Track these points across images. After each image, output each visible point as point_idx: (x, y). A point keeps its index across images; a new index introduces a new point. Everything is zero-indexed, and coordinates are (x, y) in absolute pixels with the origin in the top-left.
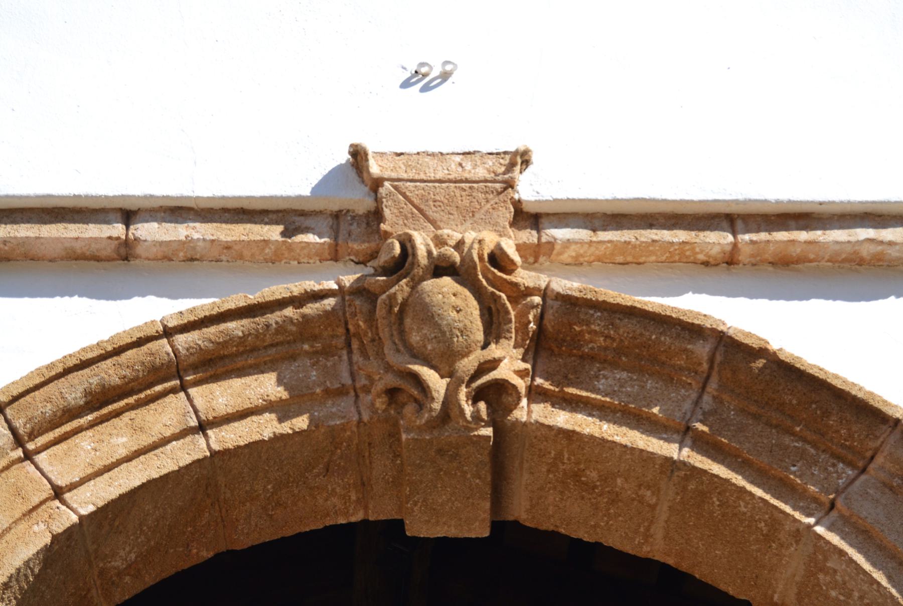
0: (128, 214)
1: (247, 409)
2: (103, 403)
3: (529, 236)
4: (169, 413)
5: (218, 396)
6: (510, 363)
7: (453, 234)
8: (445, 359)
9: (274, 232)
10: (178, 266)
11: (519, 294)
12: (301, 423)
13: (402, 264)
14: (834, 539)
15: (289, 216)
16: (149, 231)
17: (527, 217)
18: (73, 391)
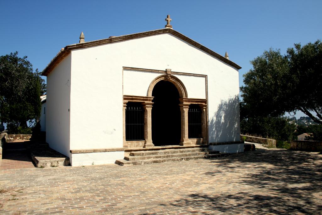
0: (159, 71)
1: (163, 79)
2: (157, 79)
4: (160, 79)
17: (171, 72)
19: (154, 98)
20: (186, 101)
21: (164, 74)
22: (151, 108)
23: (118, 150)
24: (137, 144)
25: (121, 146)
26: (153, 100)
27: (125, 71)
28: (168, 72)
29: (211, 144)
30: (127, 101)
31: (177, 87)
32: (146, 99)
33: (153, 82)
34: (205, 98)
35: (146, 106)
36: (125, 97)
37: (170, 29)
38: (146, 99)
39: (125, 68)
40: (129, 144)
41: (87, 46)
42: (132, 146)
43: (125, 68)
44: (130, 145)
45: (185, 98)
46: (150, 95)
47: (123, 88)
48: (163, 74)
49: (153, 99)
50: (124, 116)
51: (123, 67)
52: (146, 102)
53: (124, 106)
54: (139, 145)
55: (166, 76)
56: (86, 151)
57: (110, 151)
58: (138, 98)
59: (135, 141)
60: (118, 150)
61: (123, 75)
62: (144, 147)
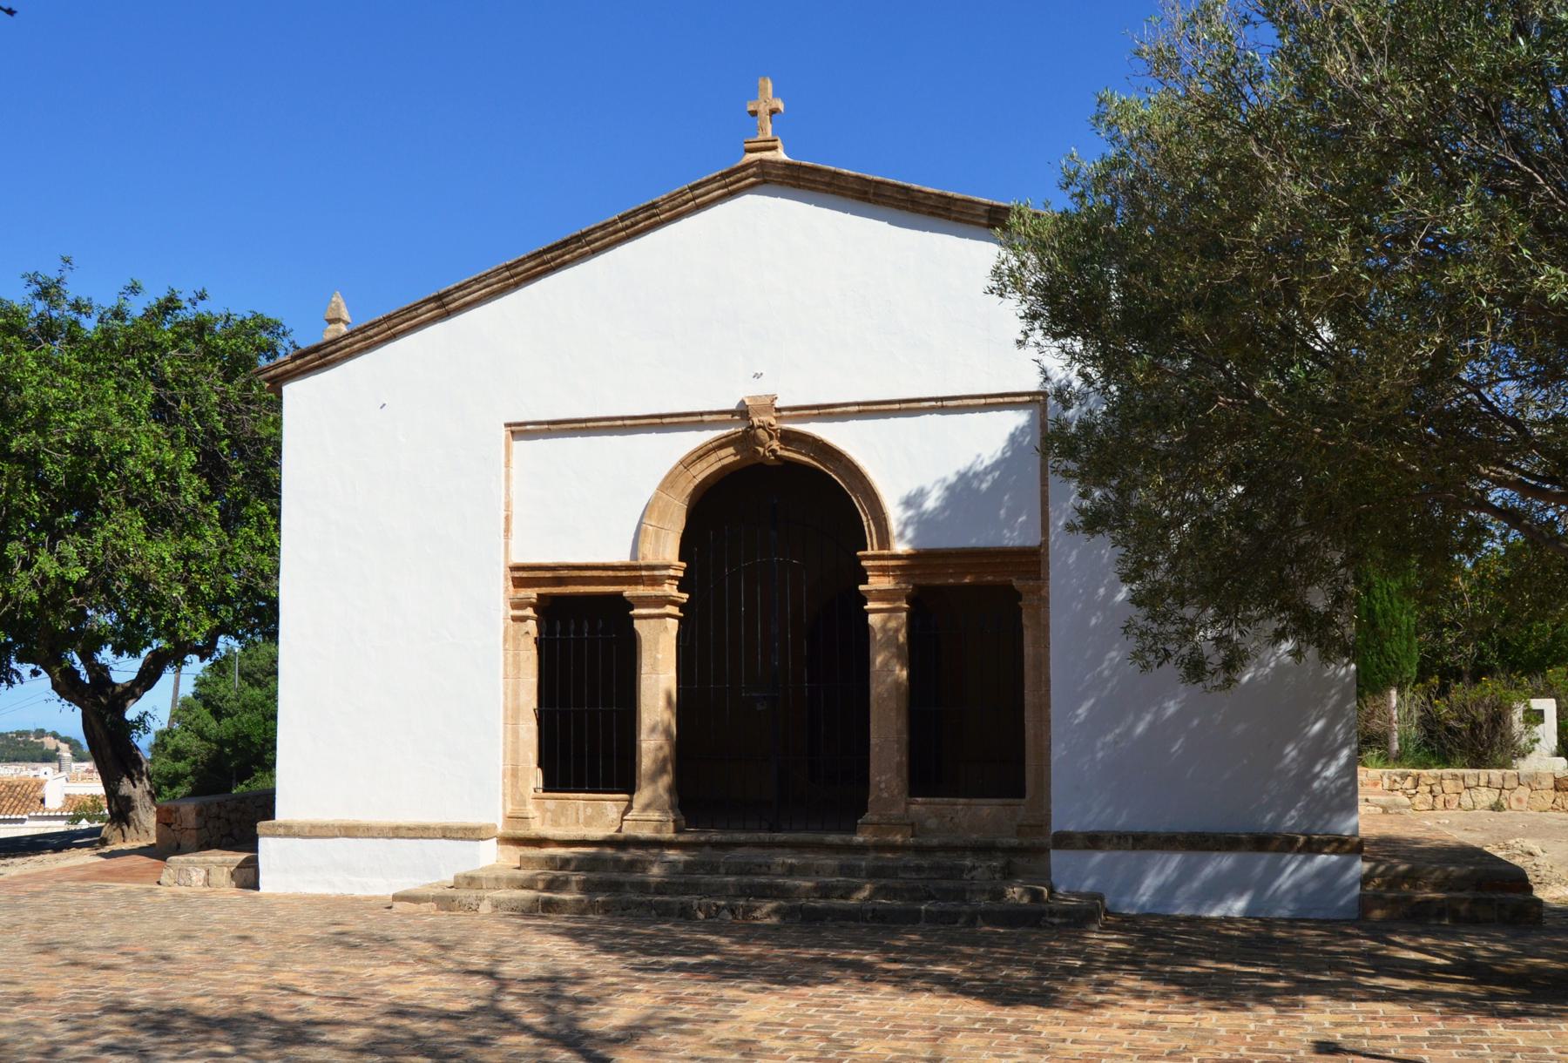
0: (701, 414)
1: (728, 456)
2: (700, 457)
4: (713, 457)
5: (722, 453)
6: (775, 444)
8: (762, 445)
9: (729, 417)
13: (752, 427)
15: (732, 413)
16: (706, 418)
17: (778, 410)
20: (884, 571)
21: (733, 430)
24: (589, 810)
27: (520, 446)
30: (532, 593)
33: (669, 483)
34: (1033, 540)
36: (517, 574)
37: (761, 160)
39: (520, 431)
42: (563, 820)
43: (520, 431)
45: (876, 552)
47: (507, 530)
48: (725, 432)
52: (629, 591)
53: (515, 619)
54: (601, 814)
55: (746, 441)
56: (313, 827)
57: (404, 833)
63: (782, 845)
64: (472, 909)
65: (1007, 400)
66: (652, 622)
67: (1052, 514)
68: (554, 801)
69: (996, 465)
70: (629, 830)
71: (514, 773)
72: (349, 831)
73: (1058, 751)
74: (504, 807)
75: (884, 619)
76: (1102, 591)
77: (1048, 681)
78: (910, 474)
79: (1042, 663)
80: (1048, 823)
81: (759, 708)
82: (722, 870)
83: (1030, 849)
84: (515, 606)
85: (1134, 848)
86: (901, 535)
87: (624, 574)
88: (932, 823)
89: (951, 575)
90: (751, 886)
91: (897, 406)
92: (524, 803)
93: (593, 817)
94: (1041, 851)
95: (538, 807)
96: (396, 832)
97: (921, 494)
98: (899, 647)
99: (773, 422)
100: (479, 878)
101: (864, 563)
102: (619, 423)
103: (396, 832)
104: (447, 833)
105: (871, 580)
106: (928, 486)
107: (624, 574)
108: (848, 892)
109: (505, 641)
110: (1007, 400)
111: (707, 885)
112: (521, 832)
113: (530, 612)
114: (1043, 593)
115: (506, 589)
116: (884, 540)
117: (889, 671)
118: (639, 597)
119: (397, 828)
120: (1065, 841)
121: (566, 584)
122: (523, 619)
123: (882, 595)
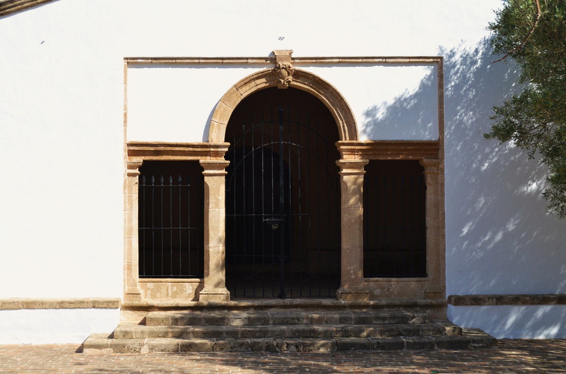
0: (247, 59)
1: (262, 83)
3: (293, 61)
4: (253, 84)
5: (258, 82)
6: (290, 78)
7: (284, 63)
8: (283, 79)
9: (264, 61)
10: (253, 65)
11: (291, 70)
12: (268, 84)
13: (279, 68)
14: (324, 98)
16: (250, 61)
17: (293, 59)
18: (243, 83)
19: (230, 148)
20: (352, 152)
21: (265, 69)
22: (223, 178)
23: (110, 305)
24: (175, 289)
25: (118, 293)
26: (226, 153)
28: (281, 60)
29: (459, 301)
30: (139, 160)
31: (328, 107)
32: (205, 149)
35: (206, 172)
36: (131, 148)
38: (205, 149)
39: (133, 62)
40: (149, 289)
41: (13, 9)
42: (158, 295)
43: (133, 62)
44: (152, 290)
46: (218, 137)
47: (125, 122)
49: (226, 149)
50: (131, 203)
51: (126, 59)
52: (203, 160)
53: (130, 175)
54: (182, 290)
57: (67, 305)
58: (177, 149)
59: (169, 280)
60: (110, 305)
61: (125, 83)
62: (196, 298)
63: (296, 306)
64: (137, 351)
65: (421, 60)
66: (216, 178)
67: (447, 123)
68: (151, 283)
69: (416, 95)
70: (203, 300)
71: (129, 267)
72: (29, 305)
73: (451, 252)
74: (125, 288)
75: (351, 179)
76: (474, 166)
77: (444, 214)
78: (370, 99)
79: (439, 205)
80: (444, 291)
81: (274, 227)
82: (271, 322)
83: (436, 304)
84: (130, 167)
85: (497, 304)
86: (364, 131)
87: (199, 150)
88: (377, 292)
89: (390, 155)
90: (298, 331)
91: (361, 60)
92: (135, 285)
93: (177, 292)
94: (441, 306)
95: (142, 287)
96: (62, 305)
97: (375, 109)
98: (360, 195)
99: (291, 66)
100: (131, 332)
101: (342, 147)
102: (197, 61)
103: (62, 305)
104: (95, 305)
105: (345, 156)
106: (379, 106)
107: (199, 150)
108: (357, 334)
109: (125, 188)
110: (421, 60)
111: (273, 332)
112: (136, 303)
113: (137, 171)
114: (441, 166)
115: (125, 158)
116: (353, 133)
117: (353, 207)
118: (209, 163)
119: (62, 302)
120: (459, 301)
121: (162, 155)
122: (133, 175)
123: (352, 165)
